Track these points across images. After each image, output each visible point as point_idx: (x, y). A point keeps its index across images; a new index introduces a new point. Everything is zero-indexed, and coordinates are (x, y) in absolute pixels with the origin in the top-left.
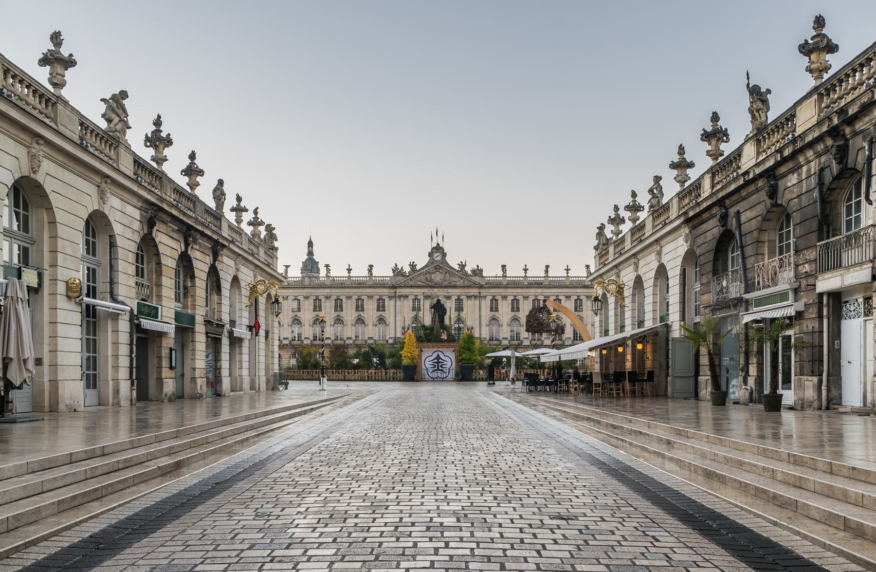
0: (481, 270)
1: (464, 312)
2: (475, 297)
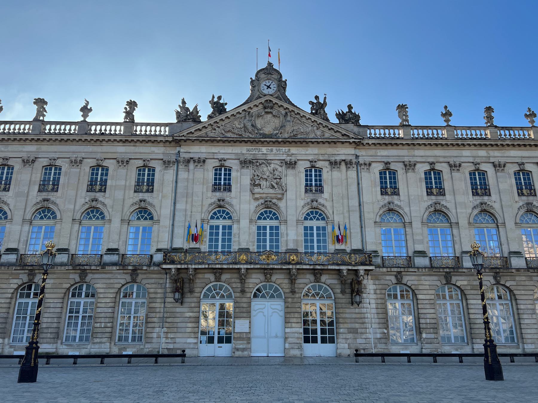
0: (356, 118)
1: (326, 195)
2: (348, 164)
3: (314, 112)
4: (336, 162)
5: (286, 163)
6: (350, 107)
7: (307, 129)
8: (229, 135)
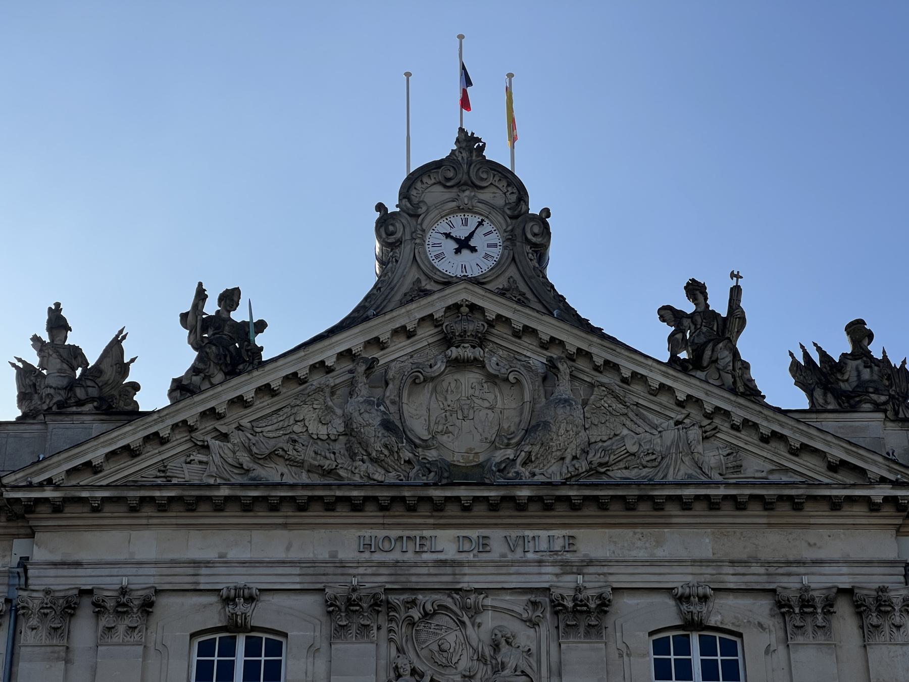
3: (683, 355)
4: (806, 602)
5: (557, 607)
6: (858, 332)
7: (651, 439)
8: (272, 472)
